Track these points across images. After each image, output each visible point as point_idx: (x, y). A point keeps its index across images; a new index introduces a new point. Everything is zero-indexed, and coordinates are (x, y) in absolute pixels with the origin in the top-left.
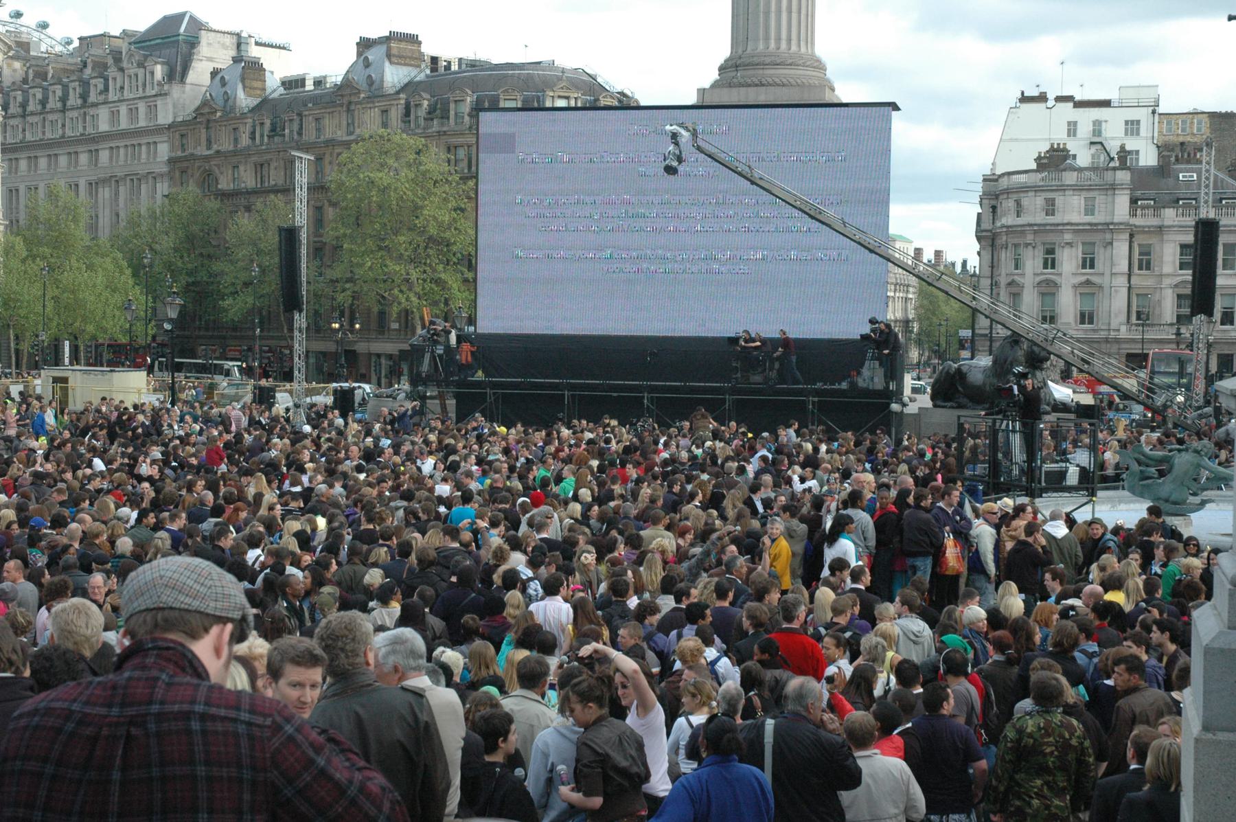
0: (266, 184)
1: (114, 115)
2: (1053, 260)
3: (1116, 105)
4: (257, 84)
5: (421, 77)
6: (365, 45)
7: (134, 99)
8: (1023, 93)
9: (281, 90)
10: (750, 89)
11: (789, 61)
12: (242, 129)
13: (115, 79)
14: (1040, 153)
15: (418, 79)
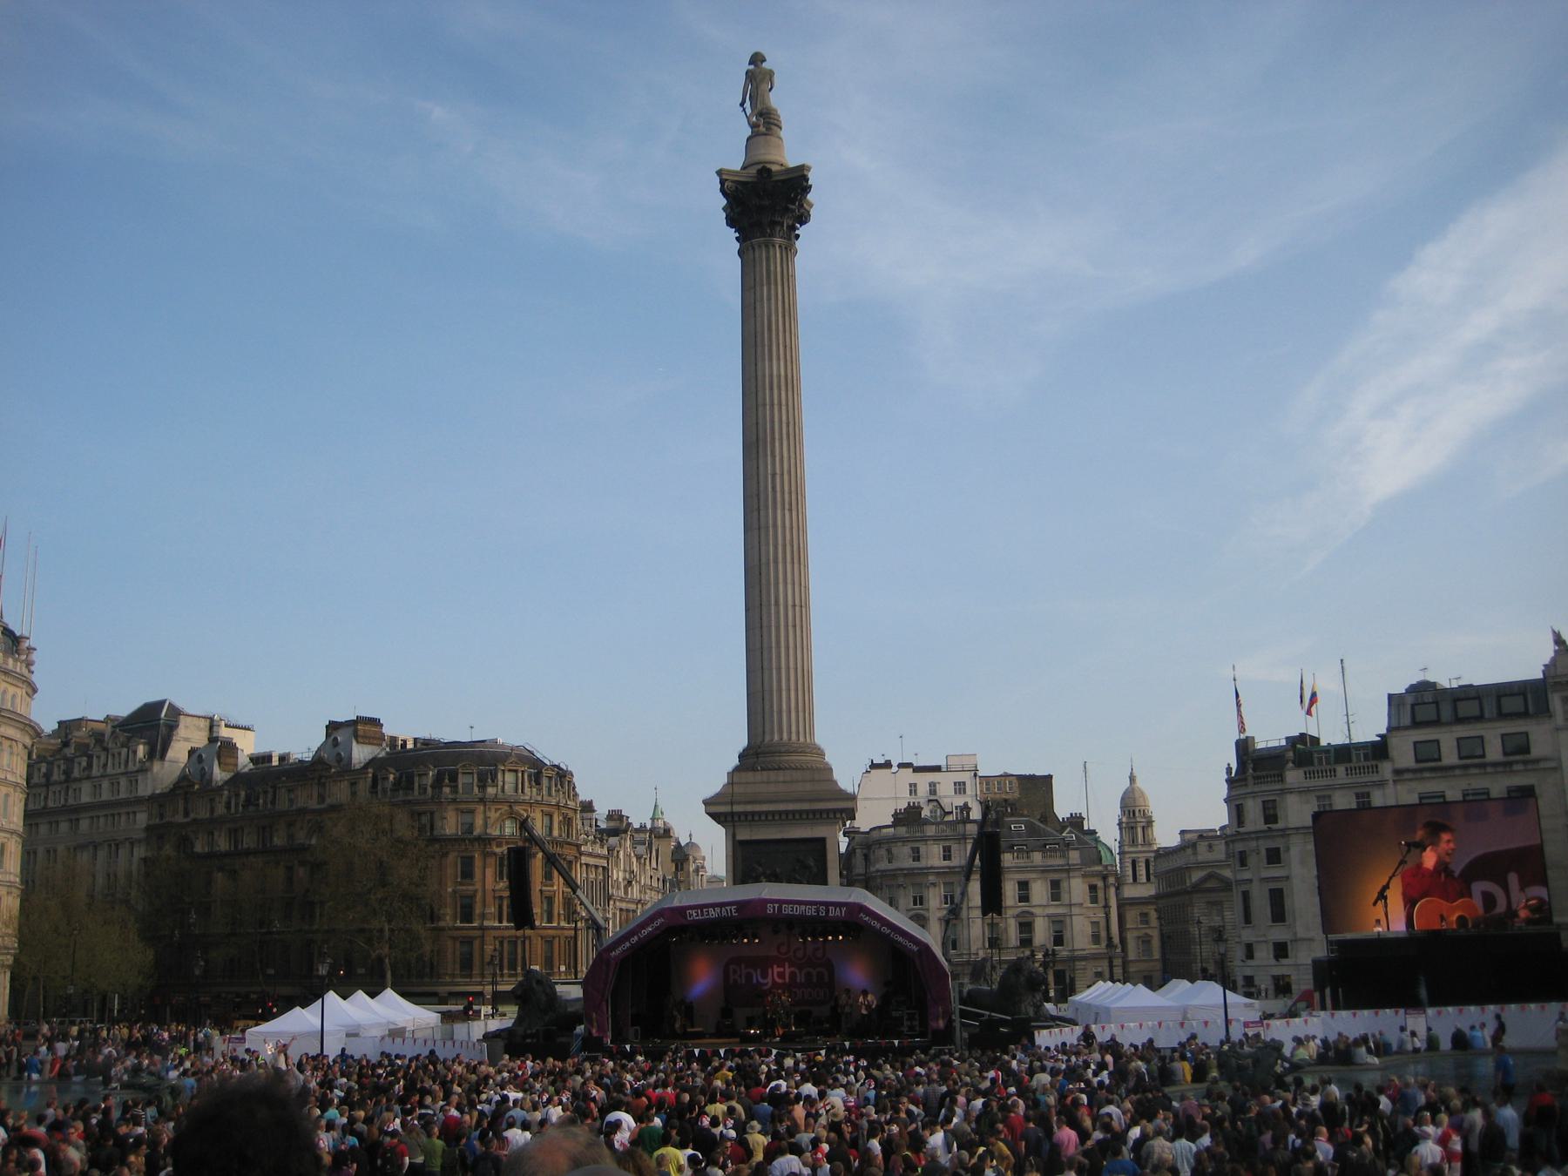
0: (240, 847)
1: (97, 788)
2: (921, 898)
3: (945, 770)
4: (231, 761)
5: (383, 754)
6: (333, 727)
7: (116, 775)
8: (872, 761)
9: (251, 766)
10: (771, 773)
11: (800, 750)
12: (217, 799)
13: (98, 757)
14: (896, 810)
15: (381, 756)
